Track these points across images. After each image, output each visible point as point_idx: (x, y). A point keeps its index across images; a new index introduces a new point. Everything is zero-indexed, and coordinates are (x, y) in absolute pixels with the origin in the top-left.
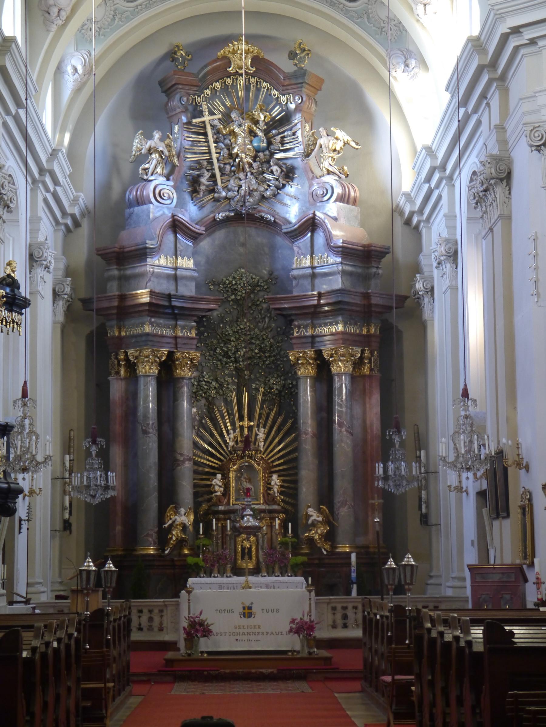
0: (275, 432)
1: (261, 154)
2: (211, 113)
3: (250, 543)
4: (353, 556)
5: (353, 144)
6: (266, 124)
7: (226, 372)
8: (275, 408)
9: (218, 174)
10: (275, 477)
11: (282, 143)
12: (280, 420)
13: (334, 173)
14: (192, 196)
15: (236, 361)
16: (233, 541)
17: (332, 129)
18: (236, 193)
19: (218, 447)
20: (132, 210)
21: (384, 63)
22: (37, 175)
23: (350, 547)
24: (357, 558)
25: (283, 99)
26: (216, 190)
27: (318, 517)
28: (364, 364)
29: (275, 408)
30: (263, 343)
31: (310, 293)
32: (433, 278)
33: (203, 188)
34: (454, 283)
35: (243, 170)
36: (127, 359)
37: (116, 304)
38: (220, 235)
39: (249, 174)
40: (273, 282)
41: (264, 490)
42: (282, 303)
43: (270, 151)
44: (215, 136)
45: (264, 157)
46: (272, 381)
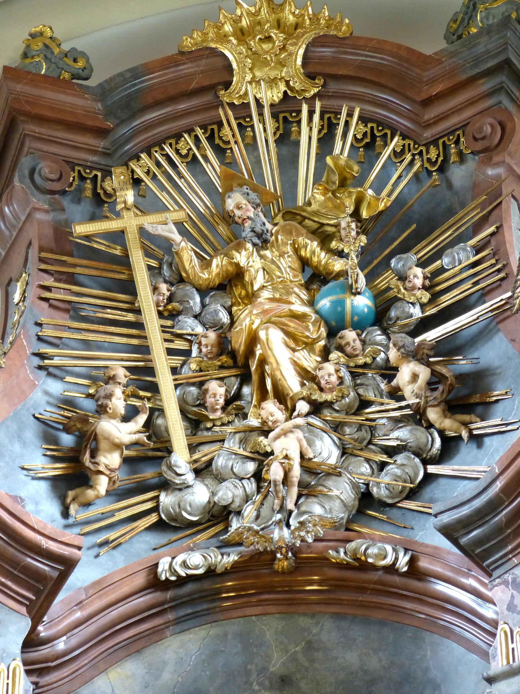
18: (251, 486)
26: (169, 475)
39: (303, 407)
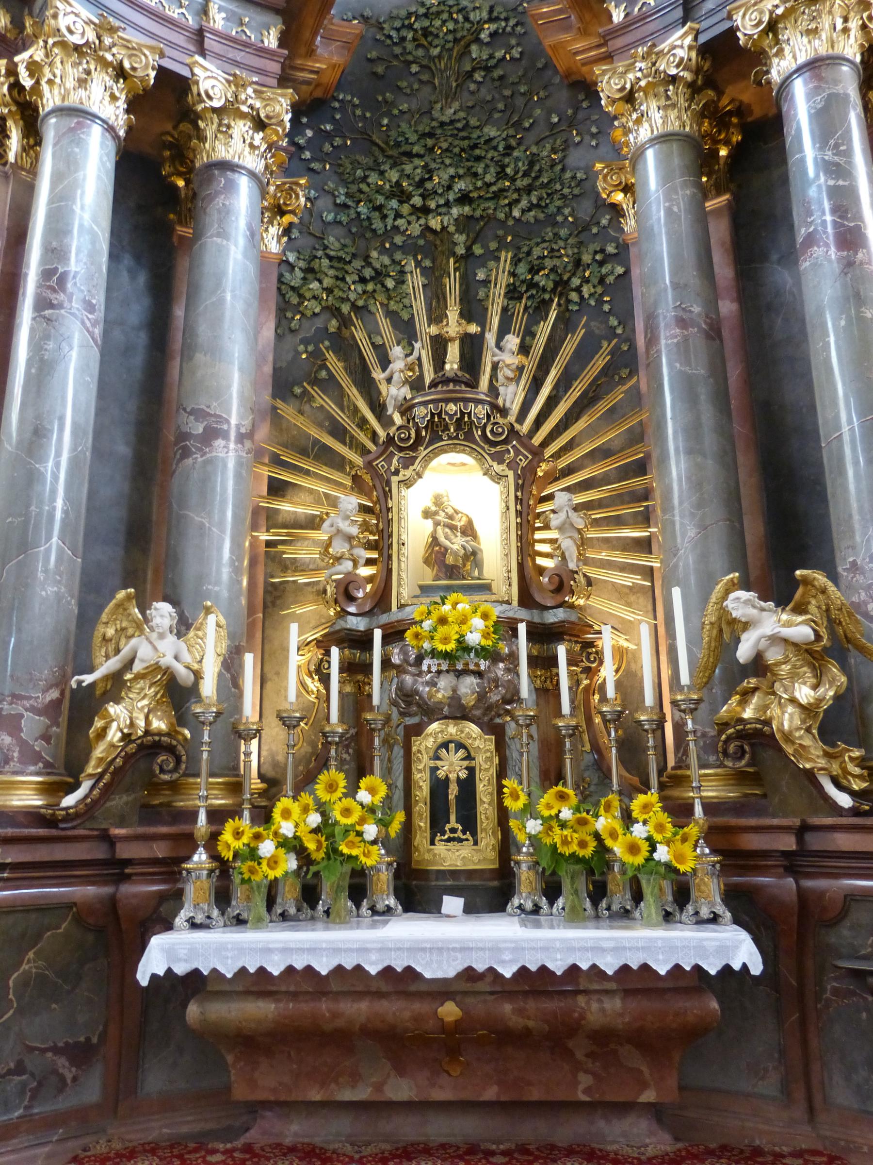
3: (469, 757)
16: (398, 752)
30: (508, 155)
46: (537, 252)
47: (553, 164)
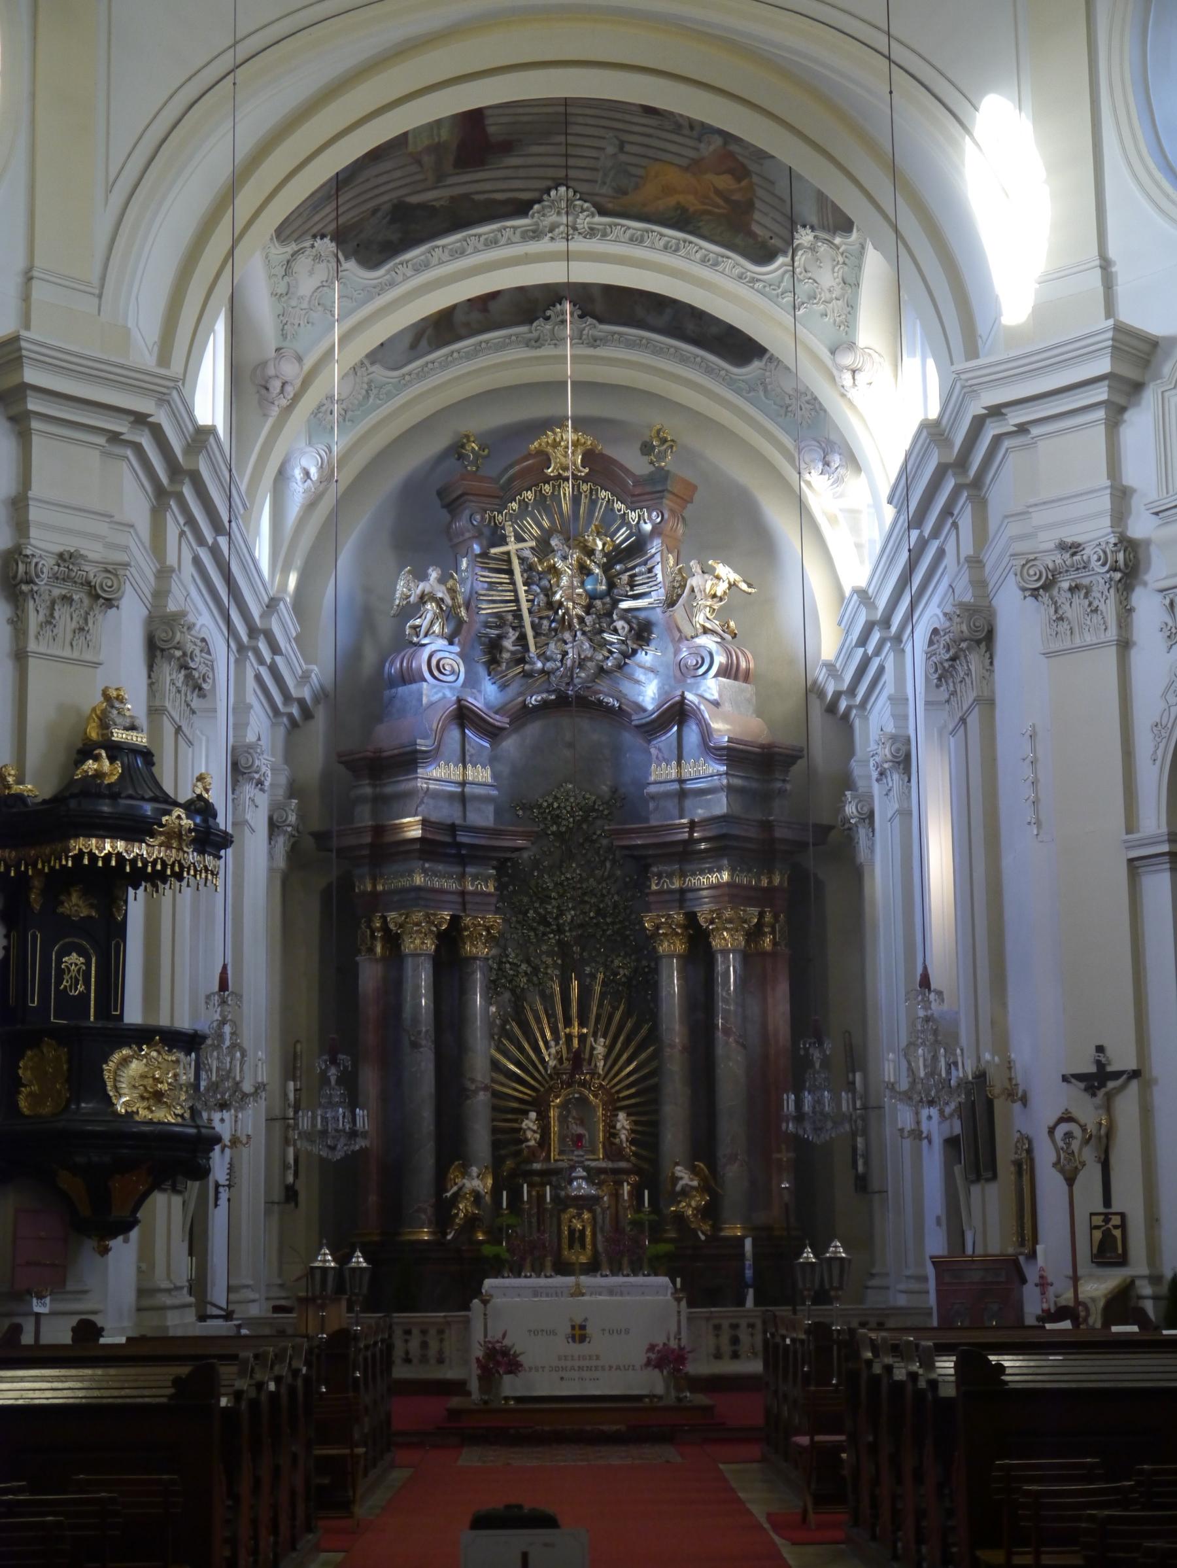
0: (623, 1044)
1: (598, 603)
2: (520, 539)
4: (748, 1243)
5: (744, 586)
6: (606, 555)
7: (544, 948)
8: (622, 1007)
9: (530, 633)
10: (622, 1116)
11: (632, 586)
12: (629, 1025)
13: (713, 632)
14: (488, 669)
15: (560, 930)
17: (710, 562)
18: (559, 664)
19: (531, 1068)
20: (394, 690)
21: (791, 459)
22: (245, 638)
23: (743, 1228)
24: (754, 1246)
25: (633, 516)
26: (527, 659)
27: (692, 1180)
28: (764, 934)
29: (622, 1007)
30: (602, 901)
31: (677, 822)
32: (872, 797)
33: (506, 655)
34: (906, 805)
35: (570, 627)
36: (385, 928)
37: (367, 839)
38: (534, 729)
40: (618, 804)
41: (604, 1136)
42: (631, 838)
43: (612, 598)
44: (525, 575)
45: (602, 607)
46: (616, 963)
47: (626, 908)
